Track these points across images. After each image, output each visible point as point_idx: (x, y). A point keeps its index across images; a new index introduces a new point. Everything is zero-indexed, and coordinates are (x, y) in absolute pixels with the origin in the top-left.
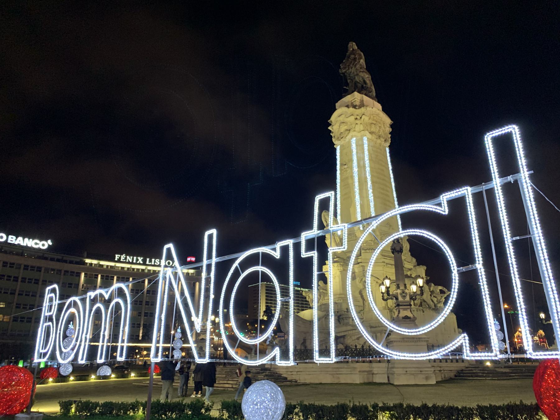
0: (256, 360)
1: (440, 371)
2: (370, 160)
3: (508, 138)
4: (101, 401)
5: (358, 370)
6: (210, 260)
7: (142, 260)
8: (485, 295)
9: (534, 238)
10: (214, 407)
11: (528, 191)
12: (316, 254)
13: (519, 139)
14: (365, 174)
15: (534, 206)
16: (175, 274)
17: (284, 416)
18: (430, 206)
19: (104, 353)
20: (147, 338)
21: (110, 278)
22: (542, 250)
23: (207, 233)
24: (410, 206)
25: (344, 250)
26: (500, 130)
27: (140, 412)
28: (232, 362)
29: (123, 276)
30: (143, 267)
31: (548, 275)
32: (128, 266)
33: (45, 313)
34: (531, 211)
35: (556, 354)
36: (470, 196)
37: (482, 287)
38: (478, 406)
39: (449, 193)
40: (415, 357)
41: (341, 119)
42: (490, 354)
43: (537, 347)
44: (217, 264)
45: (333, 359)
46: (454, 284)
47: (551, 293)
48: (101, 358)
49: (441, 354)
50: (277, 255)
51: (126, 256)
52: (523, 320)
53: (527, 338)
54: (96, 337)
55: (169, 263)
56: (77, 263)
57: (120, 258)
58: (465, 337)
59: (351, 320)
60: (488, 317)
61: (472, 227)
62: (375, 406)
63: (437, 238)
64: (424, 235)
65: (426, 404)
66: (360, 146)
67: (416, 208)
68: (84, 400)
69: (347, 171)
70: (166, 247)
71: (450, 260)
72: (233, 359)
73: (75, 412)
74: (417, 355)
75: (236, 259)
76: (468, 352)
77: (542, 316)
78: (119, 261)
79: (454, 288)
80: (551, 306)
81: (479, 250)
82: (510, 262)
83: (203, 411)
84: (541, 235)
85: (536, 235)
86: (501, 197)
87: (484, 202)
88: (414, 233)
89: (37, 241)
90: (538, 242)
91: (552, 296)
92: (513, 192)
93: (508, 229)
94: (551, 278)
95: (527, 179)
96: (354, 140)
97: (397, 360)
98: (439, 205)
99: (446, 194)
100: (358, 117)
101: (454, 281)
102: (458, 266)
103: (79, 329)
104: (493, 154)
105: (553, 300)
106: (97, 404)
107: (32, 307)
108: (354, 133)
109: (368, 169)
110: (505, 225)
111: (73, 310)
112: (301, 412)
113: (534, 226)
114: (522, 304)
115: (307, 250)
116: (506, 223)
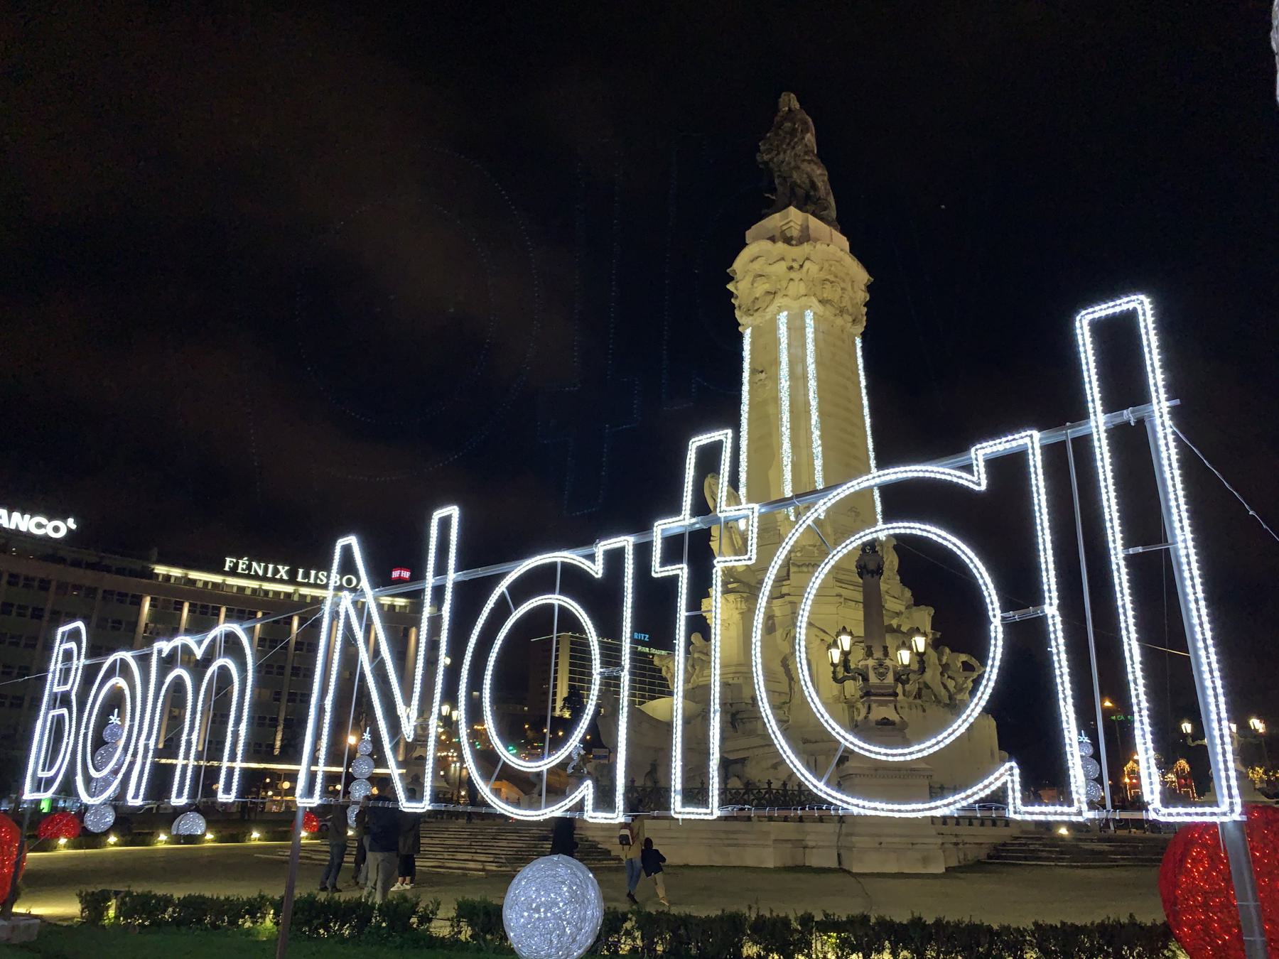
0: (539, 808)
1: (956, 844)
2: (819, 363)
3: (1128, 321)
4: (178, 893)
5: (773, 837)
6: (443, 576)
7: (287, 572)
8: (1061, 676)
9: (1176, 550)
10: (441, 914)
11: (1167, 445)
12: (686, 570)
13: (1151, 326)
14: (806, 395)
15: (1178, 479)
16: (361, 609)
17: (598, 938)
18: (947, 471)
19: (188, 782)
20: (291, 751)
21: (210, 611)
22: (1192, 578)
23: (437, 515)
24: (902, 469)
25: (749, 563)
26: (1111, 304)
27: (269, 922)
28: (484, 810)
29: (242, 607)
30: (289, 589)
31: (1203, 634)
32: (254, 584)
33: (53, 686)
34: (1171, 489)
35: (1213, 814)
36: (1038, 452)
37: (1055, 658)
38: (1036, 924)
39: (991, 443)
40: (899, 811)
41: (757, 266)
42: (1066, 809)
43: (1171, 797)
44: (458, 586)
45: (714, 810)
46: (992, 648)
47: (1207, 676)
48: (180, 794)
49: (958, 806)
50: (597, 569)
51: (250, 561)
52: (1143, 736)
53: (1150, 774)
54: (170, 747)
55: (349, 581)
56: (133, 573)
57: (236, 565)
58: (1011, 768)
59: (759, 723)
60: (1065, 725)
61: (1038, 521)
62: (806, 920)
63: (959, 543)
64: (930, 535)
65: (920, 919)
66: (797, 330)
67: (915, 474)
68: (138, 889)
69: (765, 386)
70: (341, 543)
71: (986, 594)
72: (489, 806)
73: (117, 917)
74: (903, 807)
75: (502, 576)
76: (1019, 802)
77: (1187, 727)
78: (233, 572)
79: (994, 659)
80: (1207, 704)
81: (1052, 573)
82: (1120, 603)
83: (414, 920)
84: (1190, 544)
85: (1181, 545)
86: (1107, 455)
87: (1069, 465)
88: (908, 531)
89: (43, 520)
90: (1184, 560)
91: (1208, 683)
92: (1133, 445)
93: (1118, 529)
94: (1210, 642)
95: (1166, 417)
96: (783, 318)
97: (859, 816)
98: (968, 468)
99: (985, 444)
100: (796, 265)
101: (993, 642)
102: (1004, 609)
103: (131, 727)
104: (1092, 359)
105: (1210, 692)
106: (168, 901)
107: (25, 671)
109: (812, 384)
110: (1111, 520)
111: (119, 681)
112: (638, 929)
113: (1177, 525)
114: (1143, 698)
115: (664, 562)
116: (1116, 515)
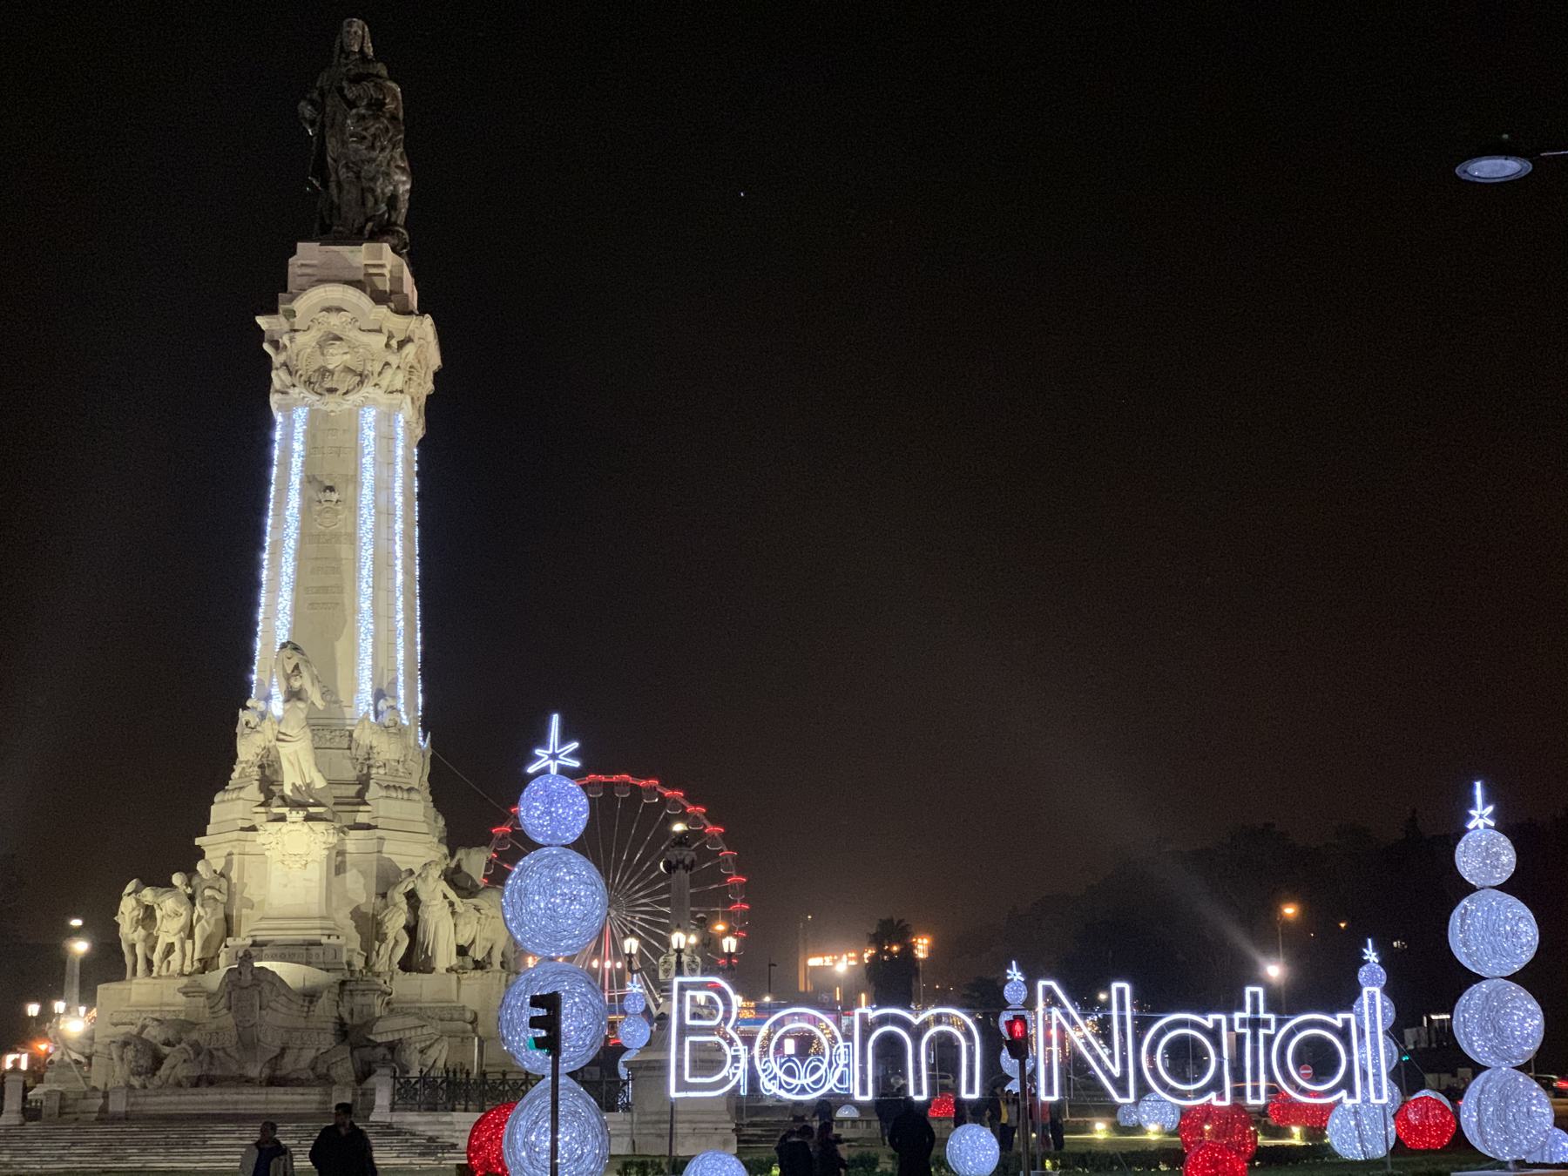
69: (337, 513)
96: (370, 415)
108: (378, 394)
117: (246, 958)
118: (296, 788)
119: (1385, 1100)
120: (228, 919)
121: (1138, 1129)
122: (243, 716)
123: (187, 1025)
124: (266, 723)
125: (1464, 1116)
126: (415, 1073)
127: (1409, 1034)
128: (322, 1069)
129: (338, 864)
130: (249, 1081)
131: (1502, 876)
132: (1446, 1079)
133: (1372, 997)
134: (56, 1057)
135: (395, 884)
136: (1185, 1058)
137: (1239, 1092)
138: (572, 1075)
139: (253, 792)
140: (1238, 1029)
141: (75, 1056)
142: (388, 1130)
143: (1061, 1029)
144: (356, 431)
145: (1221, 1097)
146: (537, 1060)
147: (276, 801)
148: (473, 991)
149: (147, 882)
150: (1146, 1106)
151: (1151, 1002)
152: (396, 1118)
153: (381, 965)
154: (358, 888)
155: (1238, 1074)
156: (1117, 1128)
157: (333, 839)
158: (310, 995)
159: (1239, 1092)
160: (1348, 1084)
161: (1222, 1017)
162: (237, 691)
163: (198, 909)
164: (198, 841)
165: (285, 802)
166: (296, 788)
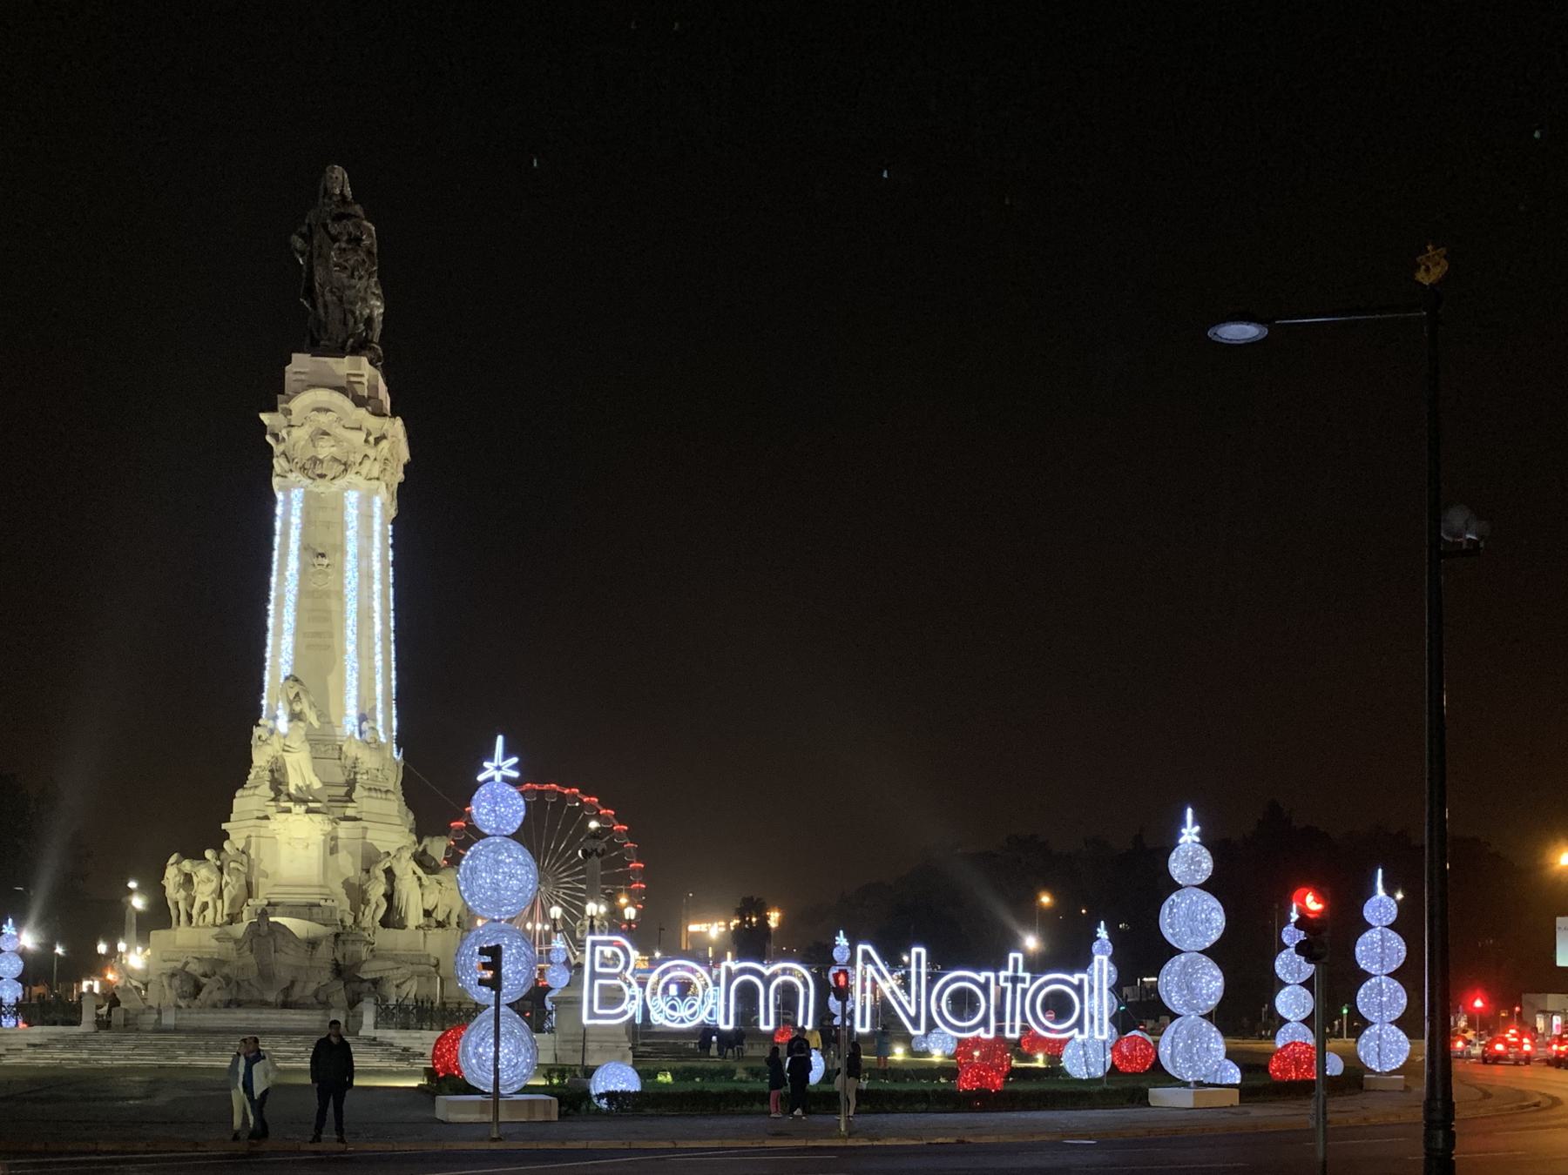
69: (327, 574)
96: (352, 497)
108: (359, 480)
117: (263, 914)
118: (299, 788)
119: (1105, 1036)
120: (249, 885)
121: (927, 1053)
122: (257, 731)
123: (222, 962)
124: (275, 737)
125: (1161, 1049)
126: (393, 1001)
127: (1126, 990)
128: (322, 997)
129: (332, 846)
130: (265, 1004)
131: (1202, 878)
132: (1150, 1024)
133: (1101, 963)
134: (121, 984)
135: (377, 862)
136: (963, 1003)
137: (1000, 1029)
138: (510, 1005)
139: (265, 790)
140: (1002, 984)
141: (135, 983)
142: (373, 1042)
143: (874, 981)
144: (340, 508)
145: (987, 1031)
146: (485, 995)
147: (283, 797)
148: (436, 943)
149: (185, 855)
150: (933, 1036)
151: (941, 961)
152: (379, 1033)
153: (366, 922)
154: (347, 865)
155: (1000, 1016)
156: (911, 1052)
157: (328, 828)
158: (313, 943)
159: (1000, 1029)
160: (1079, 1024)
161: (992, 975)
162: (252, 713)
163: (226, 877)
164: (224, 826)
165: (290, 797)
166: (299, 788)
